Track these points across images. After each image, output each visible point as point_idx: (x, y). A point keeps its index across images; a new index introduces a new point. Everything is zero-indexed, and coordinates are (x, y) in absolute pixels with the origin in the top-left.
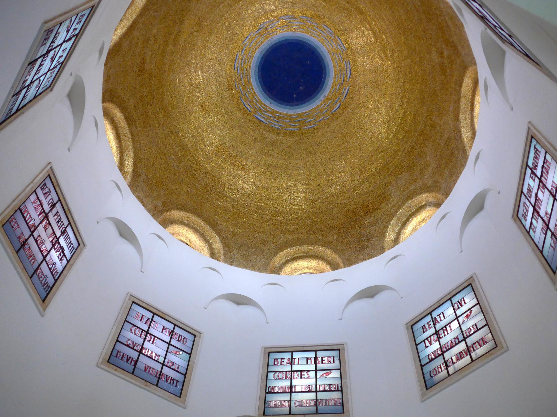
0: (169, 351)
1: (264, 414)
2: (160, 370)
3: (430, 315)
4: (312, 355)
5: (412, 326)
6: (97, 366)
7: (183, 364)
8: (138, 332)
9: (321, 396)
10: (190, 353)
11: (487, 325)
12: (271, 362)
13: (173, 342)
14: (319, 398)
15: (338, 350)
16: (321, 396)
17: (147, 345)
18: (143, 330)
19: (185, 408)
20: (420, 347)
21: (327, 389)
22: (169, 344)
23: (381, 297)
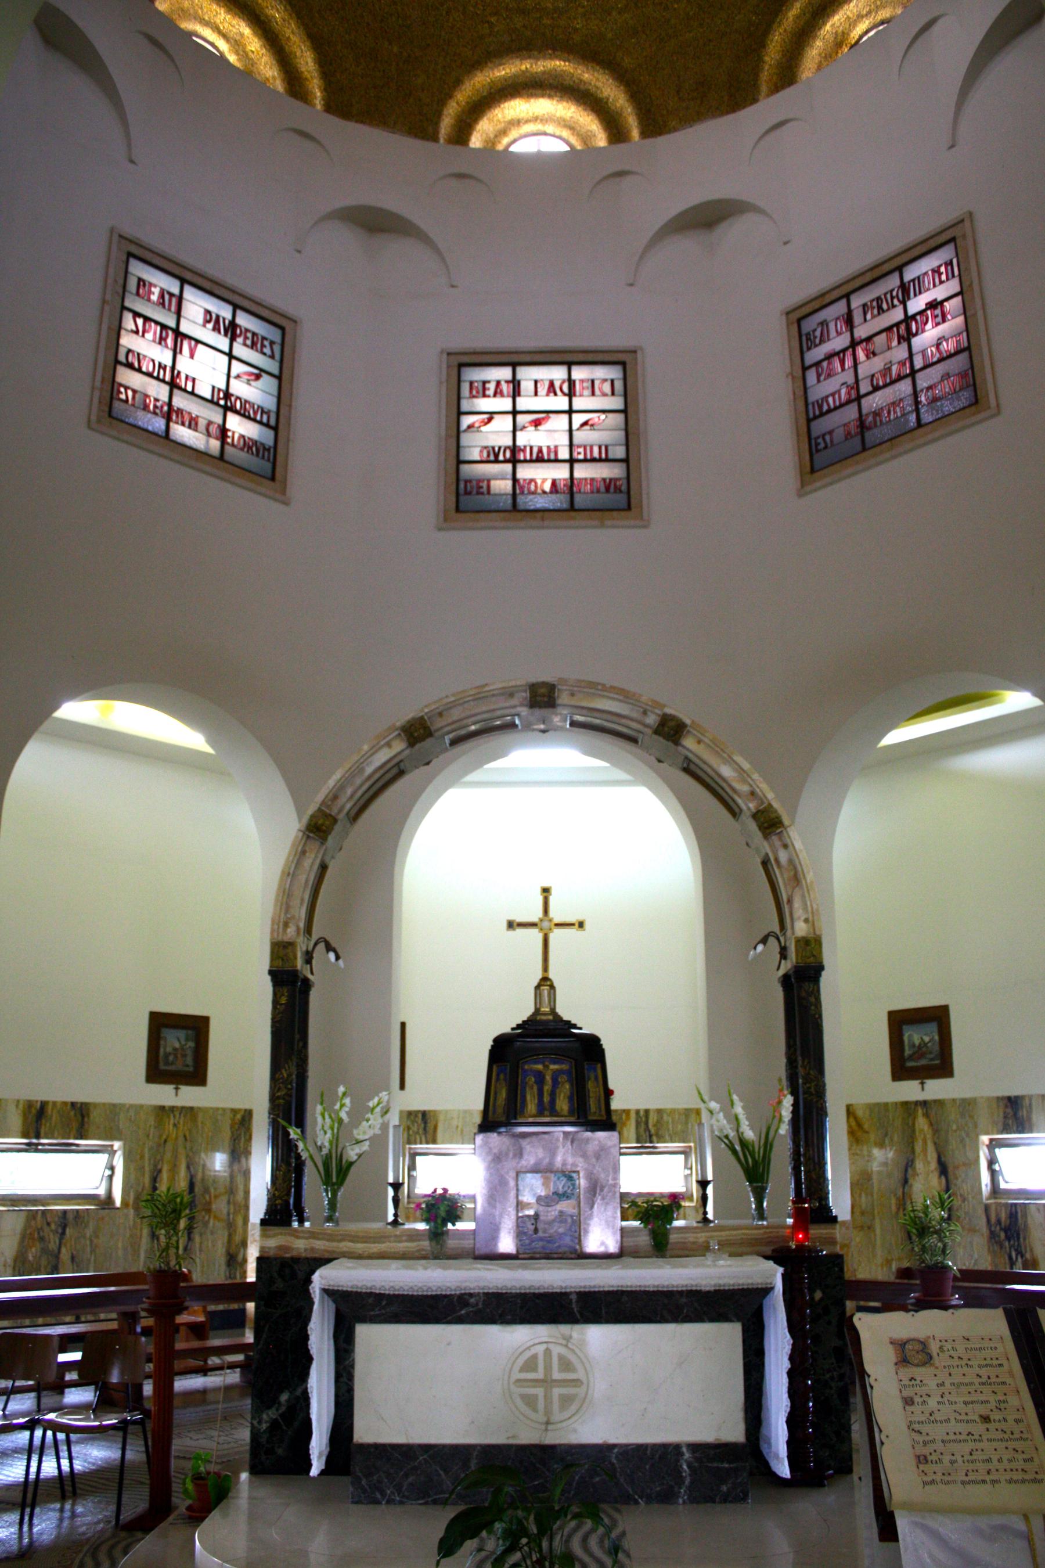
0: (233, 373)
1: (458, 510)
2: (220, 422)
3: (844, 301)
4: (558, 373)
5: (799, 321)
6: (89, 427)
7: (270, 403)
8: (154, 330)
9: (582, 472)
10: (276, 372)
11: (968, 348)
12: (465, 389)
13: (239, 350)
14: (578, 474)
15: (622, 360)
16: (582, 472)
17: (184, 365)
18: (164, 327)
19: (286, 503)
20: (811, 376)
21: (596, 454)
22: (231, 356)
23: (734, 233)
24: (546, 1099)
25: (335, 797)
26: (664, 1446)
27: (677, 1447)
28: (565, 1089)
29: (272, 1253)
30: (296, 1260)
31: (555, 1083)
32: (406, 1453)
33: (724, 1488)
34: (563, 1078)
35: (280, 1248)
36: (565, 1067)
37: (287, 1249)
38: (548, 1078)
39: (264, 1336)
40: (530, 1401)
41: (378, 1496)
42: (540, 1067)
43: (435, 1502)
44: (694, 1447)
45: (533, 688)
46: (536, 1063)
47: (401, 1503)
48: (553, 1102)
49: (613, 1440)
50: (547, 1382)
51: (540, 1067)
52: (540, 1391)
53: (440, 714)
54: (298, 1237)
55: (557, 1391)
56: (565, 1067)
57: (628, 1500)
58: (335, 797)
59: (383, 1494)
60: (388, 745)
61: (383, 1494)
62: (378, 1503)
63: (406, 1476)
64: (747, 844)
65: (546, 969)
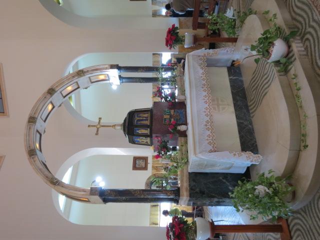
24: (144, 119)
25: (47, 177)
26: (230, 82)
27: (230, 79)
28: (141, 115)
29: (188, 193)
30: (190, 185)
31: (140, 117)
32: (241, 137)
33: (238, 71)
34: (139, 115)
35: (186, 191)
36: (136, 115)
37: (187, 189)
38: (139, 118)
39: (214, 195)
40: (224, 109)
41: (254, 145)
42: (136, 121)
43: (253, 130)
44: (229, 76)
45: (29, 122)
46: (134, 121)
47: (255, 139)
48: (145, 117)
49: (230, 91)
50: (218, 105)
51: (136, 121)
52: (221, 107)
53: (29, 147)
54: (183, 185)
55: (220, 103)
56: (136, 115)
57: (244, 89)
58: (47, 177)
59: (253, 144)
60: (34, 161)
61: (253, 144)
62: (256, 145)
63: (248, 137)
64: (86, 88)
65: (110, 126)
